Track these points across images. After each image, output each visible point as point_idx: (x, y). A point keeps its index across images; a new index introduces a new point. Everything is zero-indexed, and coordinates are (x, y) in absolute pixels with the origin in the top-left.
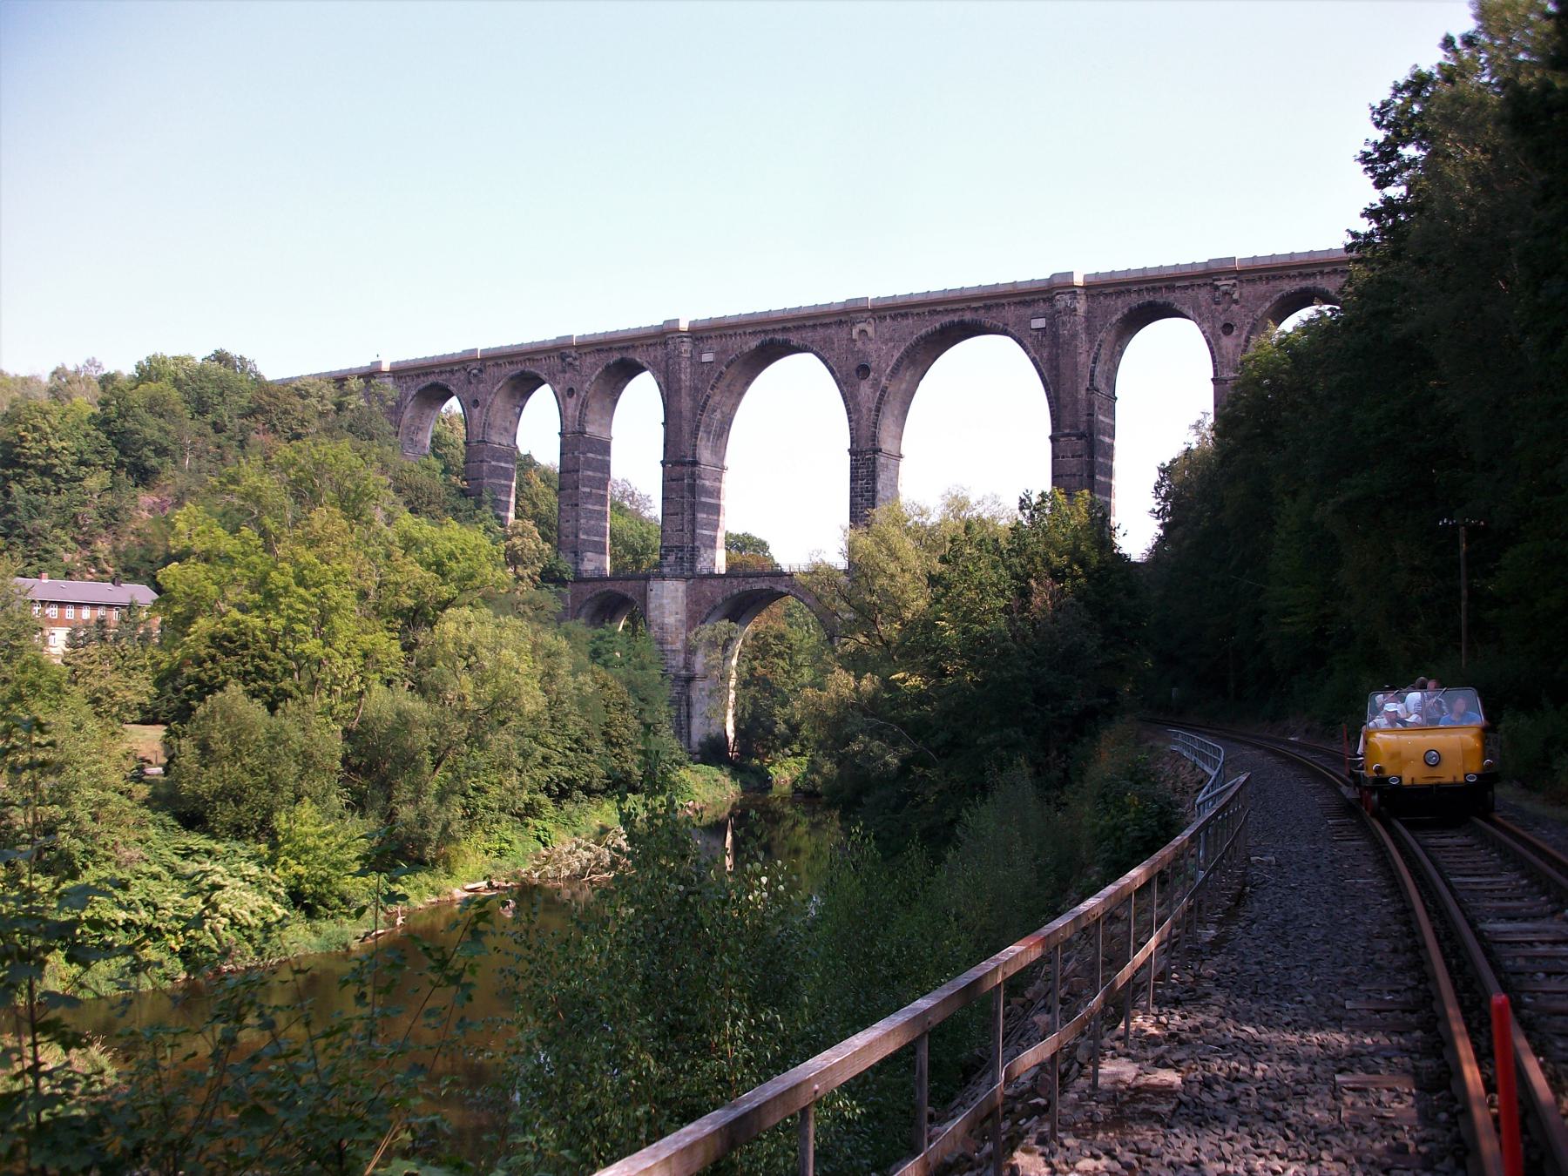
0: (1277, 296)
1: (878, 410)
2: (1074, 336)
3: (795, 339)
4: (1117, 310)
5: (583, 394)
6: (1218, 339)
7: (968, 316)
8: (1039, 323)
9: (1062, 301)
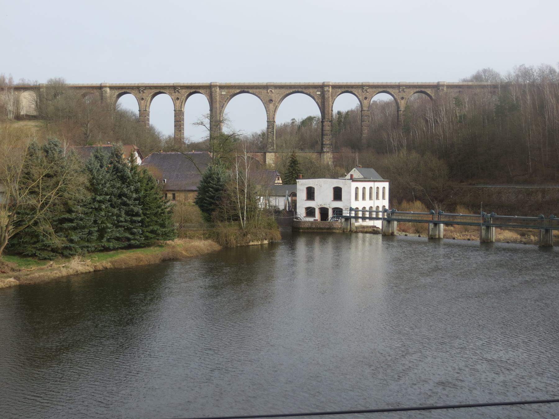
1: (275, 111)
2: (329, 97)
3: (250, 91)
5: (182, 100)
7: (300, 90)
8: (319, 93)
9: (326, 89)
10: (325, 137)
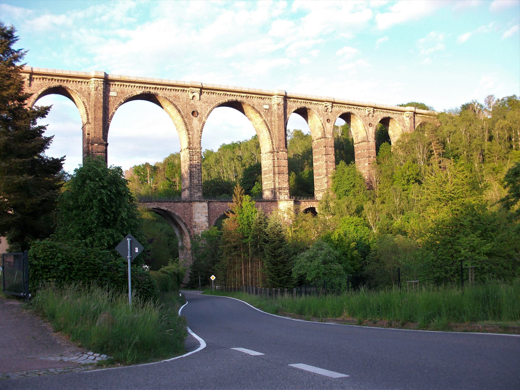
0: (341, 113)
4: (293, 107)
6: (325, 124)
10: (281, 177)
